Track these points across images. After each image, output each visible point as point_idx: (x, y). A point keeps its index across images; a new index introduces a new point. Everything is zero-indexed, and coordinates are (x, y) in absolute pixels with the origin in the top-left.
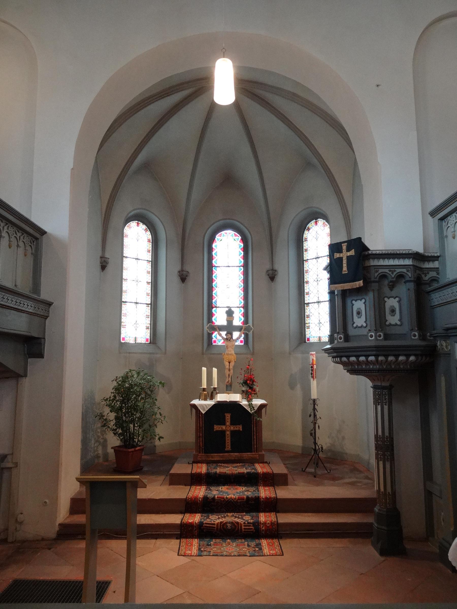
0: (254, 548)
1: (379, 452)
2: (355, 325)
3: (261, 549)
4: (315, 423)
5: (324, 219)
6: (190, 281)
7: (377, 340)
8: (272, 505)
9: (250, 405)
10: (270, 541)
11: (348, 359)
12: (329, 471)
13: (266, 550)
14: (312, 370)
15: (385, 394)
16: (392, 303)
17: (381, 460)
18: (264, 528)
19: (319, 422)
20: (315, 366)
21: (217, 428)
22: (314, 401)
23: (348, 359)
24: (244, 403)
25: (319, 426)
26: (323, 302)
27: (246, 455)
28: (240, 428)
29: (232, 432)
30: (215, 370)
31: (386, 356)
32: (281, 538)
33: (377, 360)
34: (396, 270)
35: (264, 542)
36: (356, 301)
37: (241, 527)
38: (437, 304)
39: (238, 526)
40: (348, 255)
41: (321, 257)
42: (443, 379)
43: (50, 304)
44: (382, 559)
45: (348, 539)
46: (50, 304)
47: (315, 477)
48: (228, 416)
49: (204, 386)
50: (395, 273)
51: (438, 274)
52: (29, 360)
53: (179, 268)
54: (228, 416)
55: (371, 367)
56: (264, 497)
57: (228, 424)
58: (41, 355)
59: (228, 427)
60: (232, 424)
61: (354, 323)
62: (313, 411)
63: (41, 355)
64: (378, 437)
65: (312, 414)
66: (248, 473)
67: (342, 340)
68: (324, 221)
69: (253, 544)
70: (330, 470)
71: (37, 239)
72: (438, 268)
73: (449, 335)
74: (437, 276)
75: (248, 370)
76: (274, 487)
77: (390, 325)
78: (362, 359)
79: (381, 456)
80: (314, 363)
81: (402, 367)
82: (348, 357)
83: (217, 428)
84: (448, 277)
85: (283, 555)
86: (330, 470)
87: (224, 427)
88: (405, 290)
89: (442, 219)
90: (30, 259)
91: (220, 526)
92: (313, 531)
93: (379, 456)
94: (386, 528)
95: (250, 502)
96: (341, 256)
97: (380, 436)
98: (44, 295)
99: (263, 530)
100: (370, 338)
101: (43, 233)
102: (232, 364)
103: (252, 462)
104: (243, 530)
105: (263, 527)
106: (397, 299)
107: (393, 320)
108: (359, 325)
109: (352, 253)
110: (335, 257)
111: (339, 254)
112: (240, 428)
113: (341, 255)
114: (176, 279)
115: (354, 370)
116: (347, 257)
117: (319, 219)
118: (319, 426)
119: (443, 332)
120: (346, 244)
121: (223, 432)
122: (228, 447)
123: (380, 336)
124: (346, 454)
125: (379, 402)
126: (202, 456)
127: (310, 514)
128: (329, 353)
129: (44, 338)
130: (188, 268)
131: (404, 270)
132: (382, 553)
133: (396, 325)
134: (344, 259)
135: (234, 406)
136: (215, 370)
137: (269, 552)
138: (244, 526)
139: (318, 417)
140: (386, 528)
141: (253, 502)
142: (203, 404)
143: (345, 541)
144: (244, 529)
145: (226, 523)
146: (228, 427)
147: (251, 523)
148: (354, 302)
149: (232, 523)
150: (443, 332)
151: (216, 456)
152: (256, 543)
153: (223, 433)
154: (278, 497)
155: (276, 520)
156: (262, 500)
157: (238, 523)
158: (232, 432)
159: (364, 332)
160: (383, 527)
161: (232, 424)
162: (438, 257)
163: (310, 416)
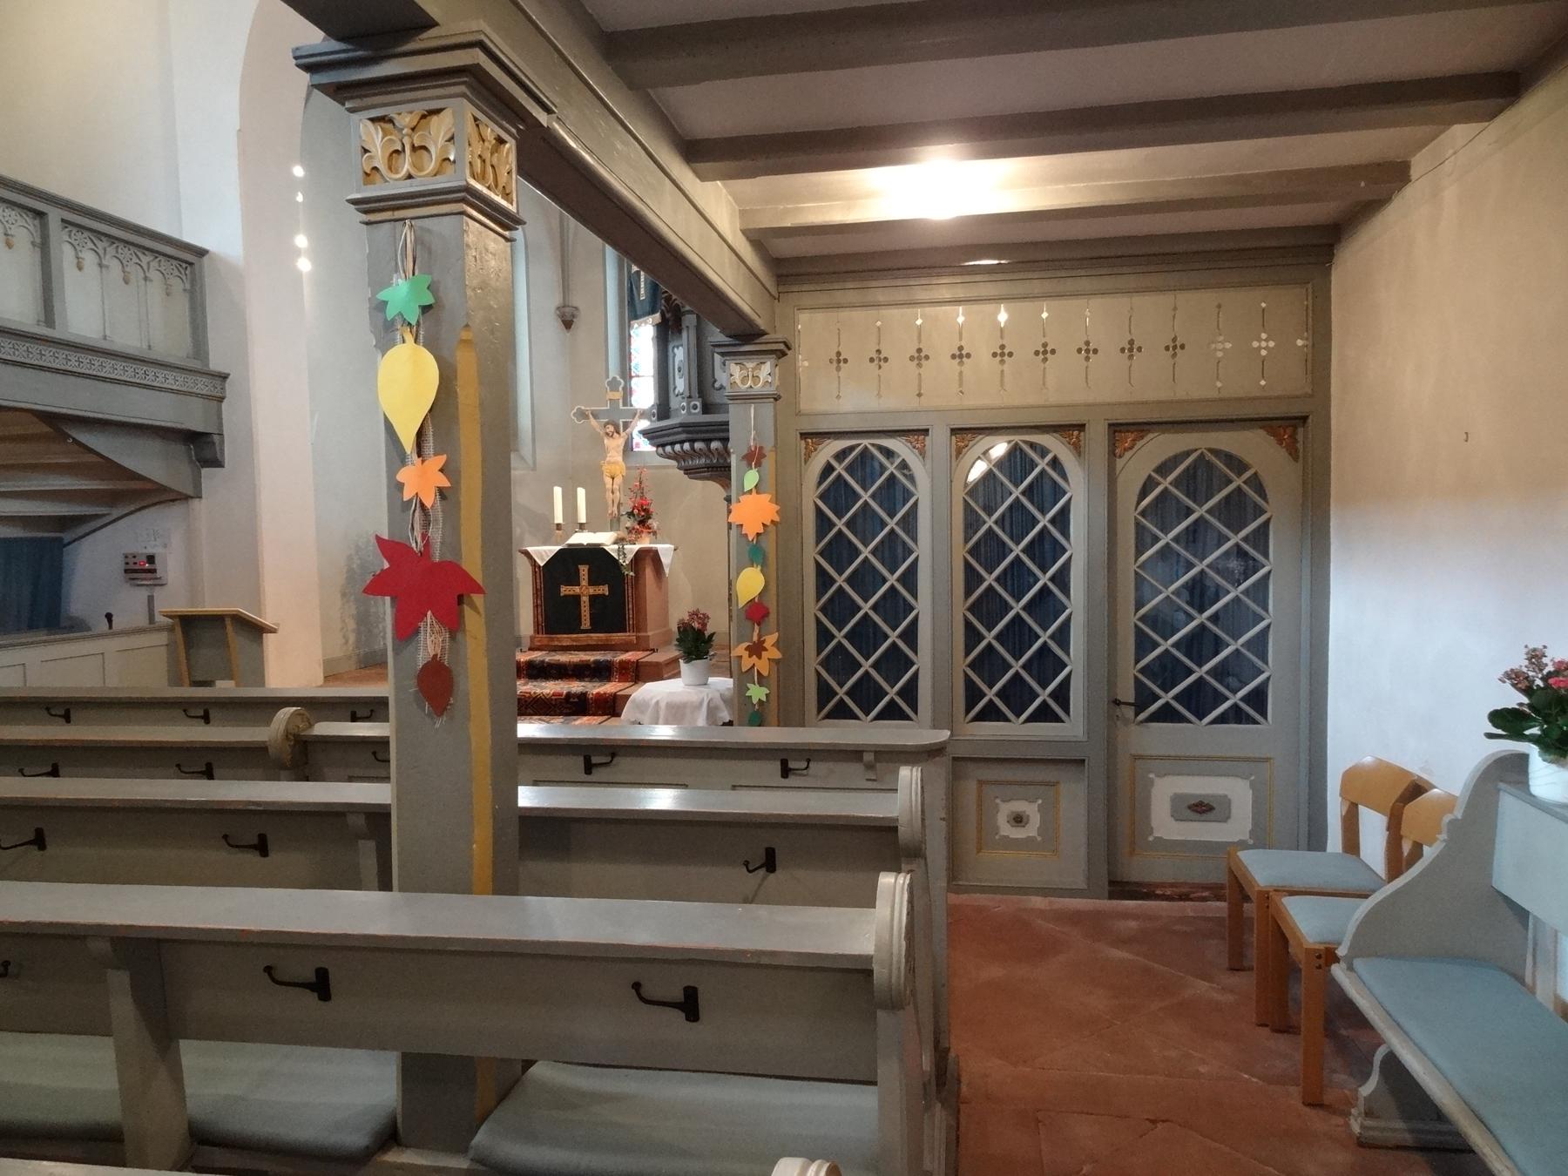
6: (581, 324)
9: (621, 551)
21: (565, 590)
24: (612, 549)
27: (617, 637)
28: (604, 590)
29: (593, 598)
30: (581, 492)
31: (708, 441)
33: (692, 448)
43: (224, 377)
46: (224, 377)
48: (584, 570)
49: (559, 519)
52: (205, 471)
53: (556, 300)
54: (584, 570)
57: (584, 583)
58: (217, 463)
59: (584, 589)
60: (592, 583)
63: (217, 463)
66: (596, 662)
71: (191, 264)
75: (641, 490)
83: (565, 590)
87: (577, 589)
90: (181, 305)
98: (215, 364)
101: (201, 253)
102: (618, 480)
103: (626, 648)
112: (604, 590)
114: (553, 325)
121: (577, 598)
122: (586, 623)
123: (695, 407)
126: (543, 638)
129: (221, 435)
130: (577, 300)
135: (595, 554)
136: (581, 492)
142: (544, 552)
146: (584, 589)
151: (566, 639)
153: (577, 598)
158: (593, 598)
161: (592, 583)
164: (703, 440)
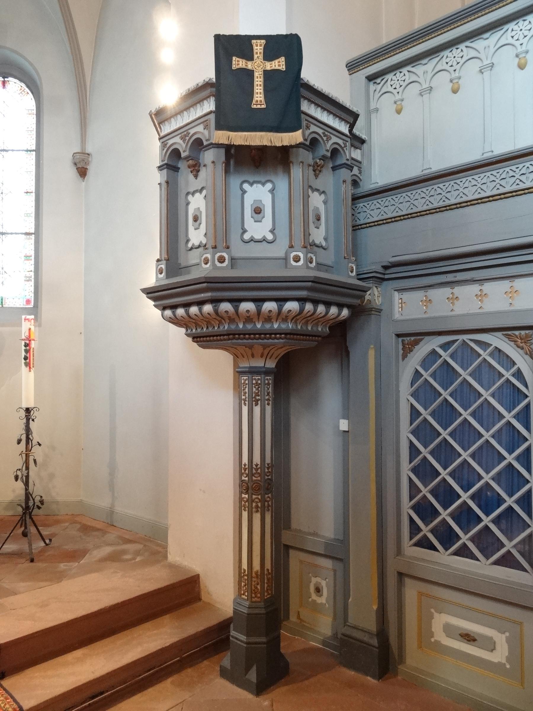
1: (254, 497)
2: (247, 237)
4: (27, 456)
5: (21, 81)
7: (308, 267)
11: (236, 308)
12: (47, 541)
14: (27, 351)
15: (268, 384)
16: (316, 200)
17: (257, 511)
19: (37, 452)
20: (33, 342)
22: (28, 410)
23: (236, 308)
25: (35, 461)
26: (12, 234)
36: (251, 184)
38: (362, 222)
41: (13, 150)
42: (372, 353)
44: (265, 701)
45: (170, 680)
47: (32, 561)
51: (360, 173)
55: (276, 326)
61: (244, 231)
62: (24, 432)
64: (252, 467)
65: (24, 438)
67: (224, 265)
68: (23, 85)
70: (50, 540)
72: (360, 163)
73: (386, 277)
74: (359, 175)
78: (270, 306)
79: (257, 502)
80: (32, 337)
81: (320, 329)
82: (236, 301)
84: (373, 181)
86: (50, 540)
89: (371, 78)
92: (102, 693)
93: (254, 504)
94: (264, 639)
97: (245, 465)
100: (294, 264)
106: (323, 197)
107: (318, 235)
108: (258, 237)
109: (279, 64)
110: (234, 67)
111: (244, 61)
115: (204, 337)
116: (266, 72)
117: (10, 79)
118: (35, 461)
119: (381, 270)
120: (263, 42)
124: (57, 503)
125: (258, 400)
127: (78, 653)
128: (154, 299)
132: (261, 688)
134: (256, 74)
139: (35, 442)
140: (264, 639)
143: (167, 684)
148: (246, 186)
150: (381, 270)
159: (279, 250)
162: (363, 142)
163: (19, 442)
164: (230, 300)
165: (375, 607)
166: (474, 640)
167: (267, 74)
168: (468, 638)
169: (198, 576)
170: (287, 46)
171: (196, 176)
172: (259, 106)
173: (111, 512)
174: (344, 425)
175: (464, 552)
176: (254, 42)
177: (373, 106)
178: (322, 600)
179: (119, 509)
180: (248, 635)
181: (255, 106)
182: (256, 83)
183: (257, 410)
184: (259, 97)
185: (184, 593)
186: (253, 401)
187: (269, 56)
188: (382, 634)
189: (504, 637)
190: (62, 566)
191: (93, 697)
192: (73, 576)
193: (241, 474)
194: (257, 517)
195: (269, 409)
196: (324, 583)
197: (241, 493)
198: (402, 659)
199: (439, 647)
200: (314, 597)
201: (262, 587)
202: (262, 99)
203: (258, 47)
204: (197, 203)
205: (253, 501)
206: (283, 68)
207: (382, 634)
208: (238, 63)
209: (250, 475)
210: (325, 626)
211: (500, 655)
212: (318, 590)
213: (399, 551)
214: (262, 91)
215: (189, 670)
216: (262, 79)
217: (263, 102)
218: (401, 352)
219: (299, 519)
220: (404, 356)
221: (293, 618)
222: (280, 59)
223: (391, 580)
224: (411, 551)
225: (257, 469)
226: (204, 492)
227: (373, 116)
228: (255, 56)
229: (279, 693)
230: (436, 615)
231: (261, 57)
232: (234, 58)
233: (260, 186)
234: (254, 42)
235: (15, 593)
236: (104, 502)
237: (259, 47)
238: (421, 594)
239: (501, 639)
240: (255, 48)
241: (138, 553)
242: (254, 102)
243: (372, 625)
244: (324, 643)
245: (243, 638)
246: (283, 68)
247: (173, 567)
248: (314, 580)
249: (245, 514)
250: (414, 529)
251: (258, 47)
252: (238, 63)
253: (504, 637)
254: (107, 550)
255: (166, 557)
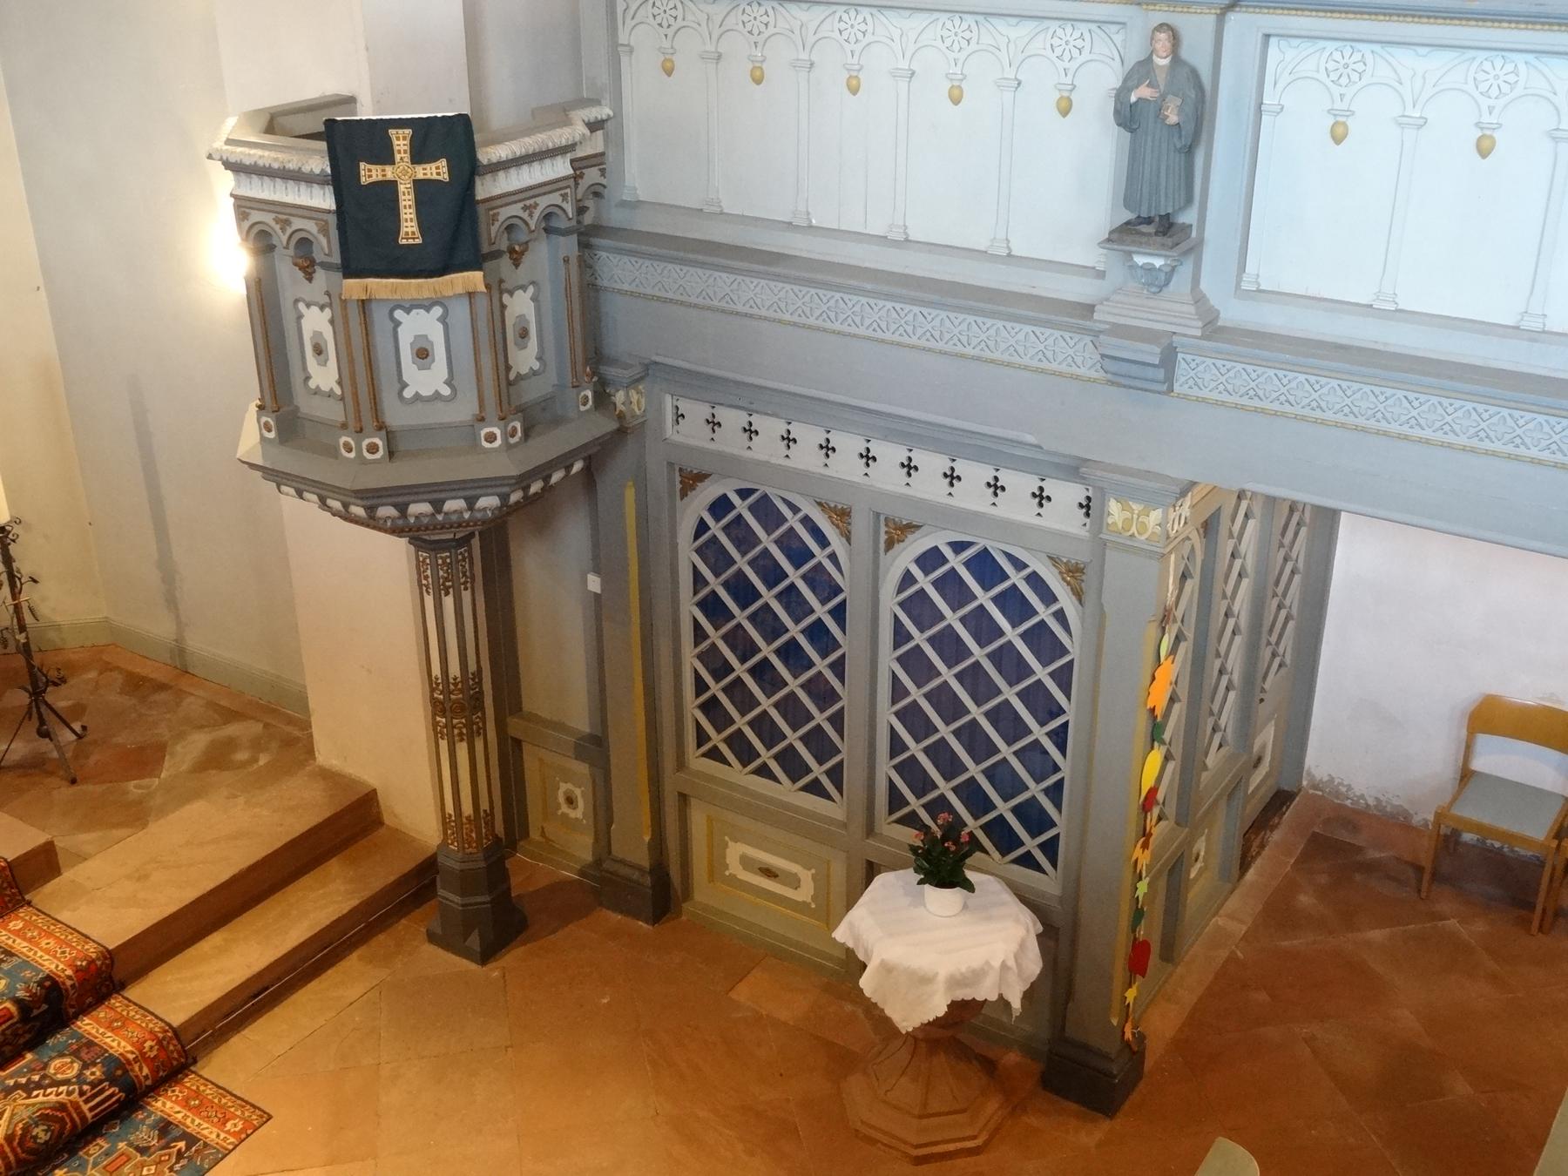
0: (167, 1146)
3: (191, 1140)
8: (105, 978)
10: (177, 1091)
13: (209, 1132)
18: (146, 1071)
32: (195, 1062)
34: (538, 200)
35: (166, 1105)
37: (77, 1107)
39: (69, 1115)
40: (420, 176)
42: (630, 494)
44: (493, 971)
45: (355, 955)
47: (74, 782)
50: (537, 213)
51: (603, 172)
56: (69, 972)
61: (404, 386)
69: (144, 1133)
72: (603, 154)
76: (29, 903)
77: (520, 377)
85: (270, 1117)
88: (545, 259)
91: (13, 1150)
94: (487, 898)
95: (36, 1012)
96: (390, 176)
99: (146, 1077)
100: (486, 445)
104: (89, 1115)
105: (141, 1069)
107: (525, 359)
109: (437, 170)
113: (390, 173)
120: (408, 132)
124: (58, 628)
127: (216, 938)
131: (555, 198)
133: (534, 373)
134: (401, 188)
137: (228, 1132)
138: (86, 1102)
140: (487, 898)
141: (45, 1007)
143: (353, 961)
144: (91, 1109)
145: (26, 1130)
147: (101, 1082)
149: (44, 1118)
152: (152, 1127)
154: (111, 945)
155: (161, 1024)
156: (69, 983)
157: (61, 1107)
160: (480, 899)
165: (647, 838)
166: (776, 876)
167: (420, 186)
168: (769, 873)
169: (374, 791)
170: (449, 138)
171: (310, 279)
172: (411, 241)
173: (180, 651)
174: (594, 584)
175: (764, 771)
176: (392, 132)
177: (622, 39)
178: (577, 814)
179: (197, 643)
180: (462, 896)
181: (404, 242)
182: (402, 204)
183: (449, 602)
184: (409, 228)
185: (355, 821)
186: (440, 591)
187: (418, 157)
188: (659, 871)
189: (809, 873)
190: (133, 788)
191: (256, 996)
192: (162, 812)
193: (432, 690)
194: (462, 750)
195: (466, 596)
196: (578, 792)
197: (434, 715)
198: (687, 894)
199: (733, 881)
200: (565, 809)
201: (479, 833)
202: (415, 229)
203: (401, 141)
204: (316, 322)
205: (454, 727)
206: (445, 177)
207: (659, 871)
208: (370, 173)
209: (447, 692)
210: (582, 848)
211: (805, 893)
212: (570, 801)
213: (681, 764)
214: (413, 216)
215: (381, 937)
216: (412, 197)
217: (418, 234)
218: (679, 486)
219: (535, 699)
220: (684, 494)
221: (534, 834)
222: (438, 163)
223: (667, 807)
224: (698, 762)
225: (455, 684)
226: (369, 671)
227: (624, 59)
228: (398, 157)
229: (512, 958)
230: (731, 844)
231: (407, 157)
232: (362, 165)
233: (422, 311)
234: (392, 132)
235: (82, 858)
236: (160, 628)
237: (401, 142)
238: (710, 820)
239: (806, 876)
240: (395, 142)
241: (257, 745)
242: (402, 234)
243: (643, 858)
244: (582, 873)
245: (457, 899)
246: (445, 177)
247: (330, 778)
248: (564, 787)
249: (444, 744)
250: (702, 737)
251: (401, 141)
252: (370, 173)
253: (809, 873)
254: (198, 742)
255: (310, 752)
